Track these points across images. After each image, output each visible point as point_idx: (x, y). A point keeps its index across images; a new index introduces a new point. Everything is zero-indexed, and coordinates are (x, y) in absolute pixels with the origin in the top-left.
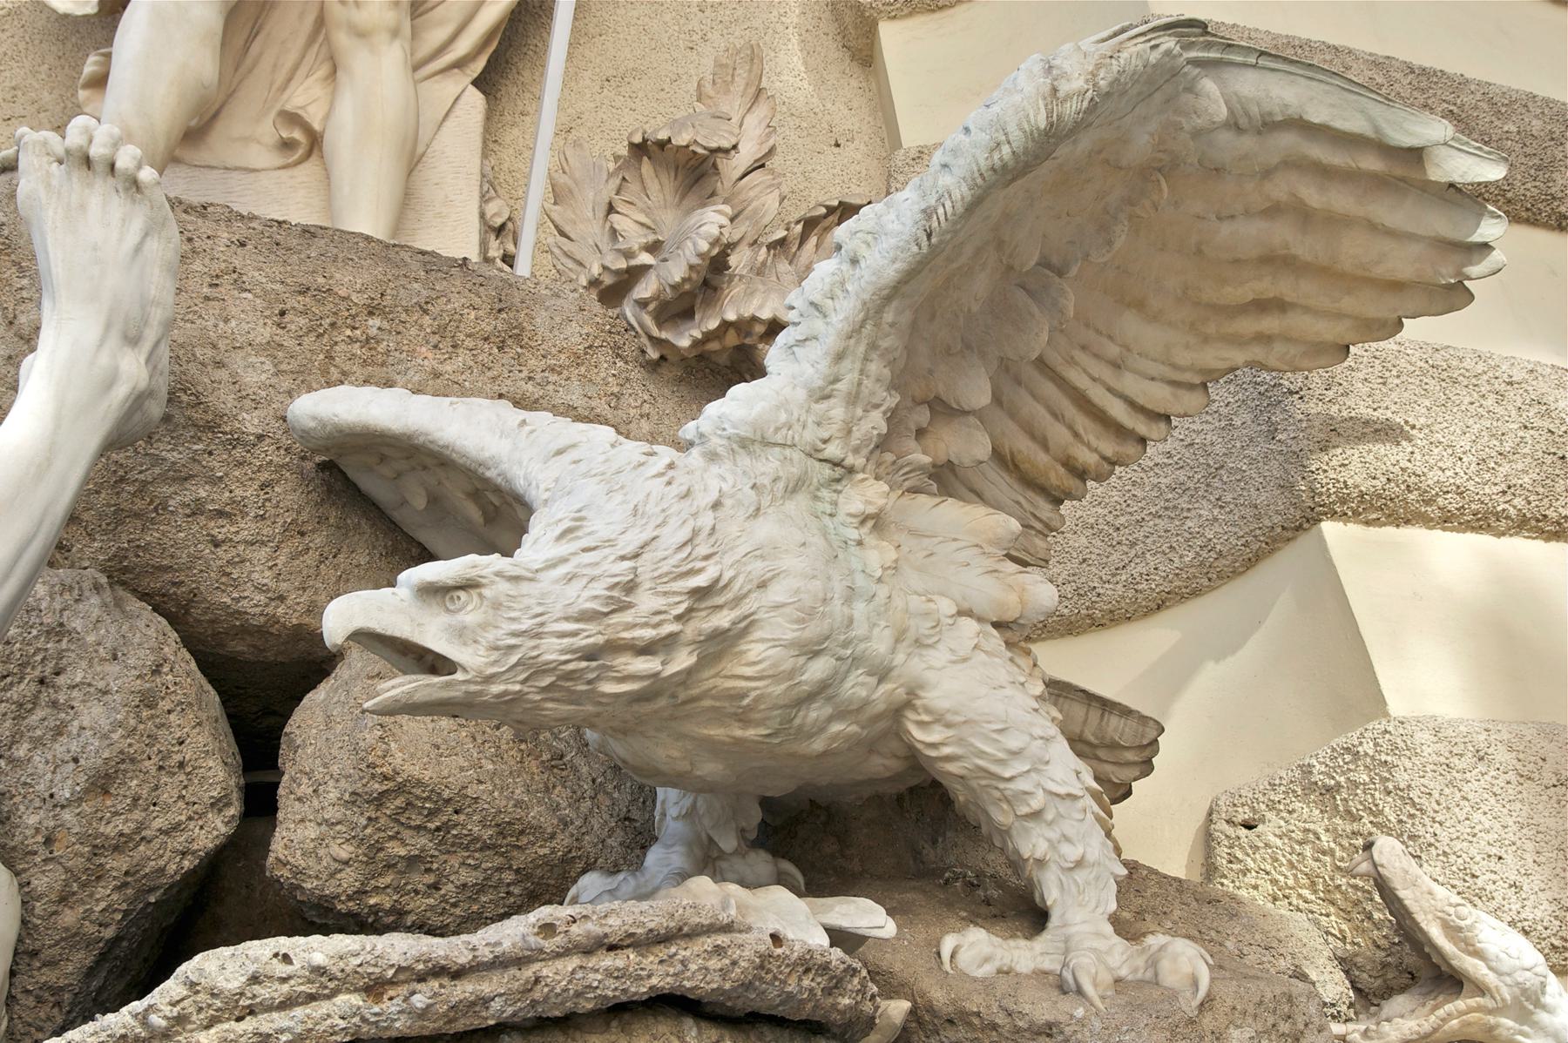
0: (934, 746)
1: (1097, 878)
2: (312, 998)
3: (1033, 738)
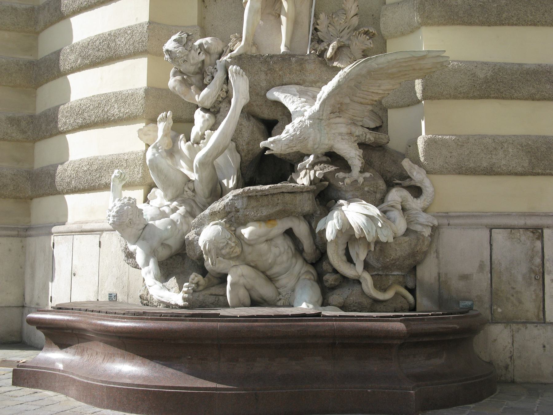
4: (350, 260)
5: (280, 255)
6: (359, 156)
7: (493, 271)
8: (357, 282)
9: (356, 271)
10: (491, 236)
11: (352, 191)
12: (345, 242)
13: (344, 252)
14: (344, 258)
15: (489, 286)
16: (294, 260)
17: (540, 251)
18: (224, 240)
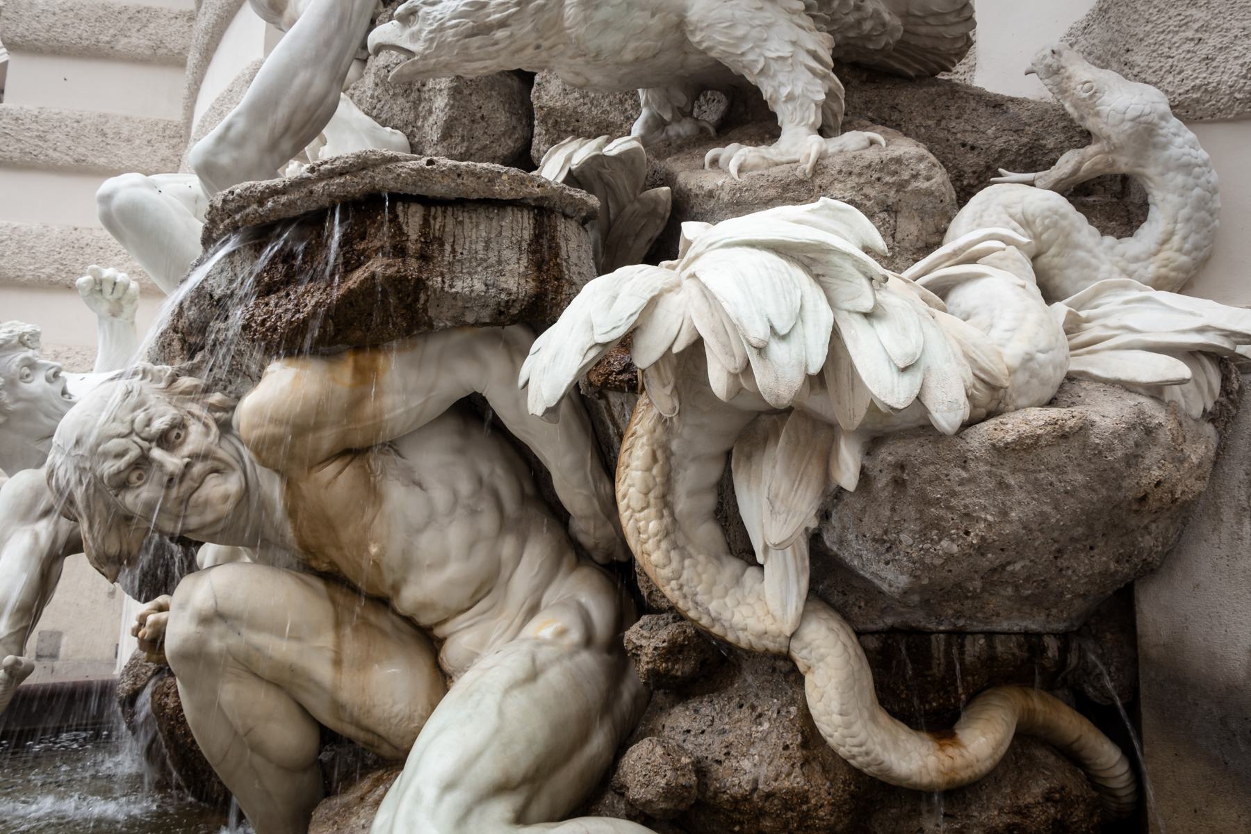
0: (700, 43)
1: (801, 105)
2: (244, 208)
3: (753, 27)
4: (740, 549)
5: (427, 525)
6: (815, 56)
8: (783, 670)
9: (763, 605)
12: (718, 447)
13: (710, 501)
14: (707, 532)
16: (508, 547)
18: (114, 445)
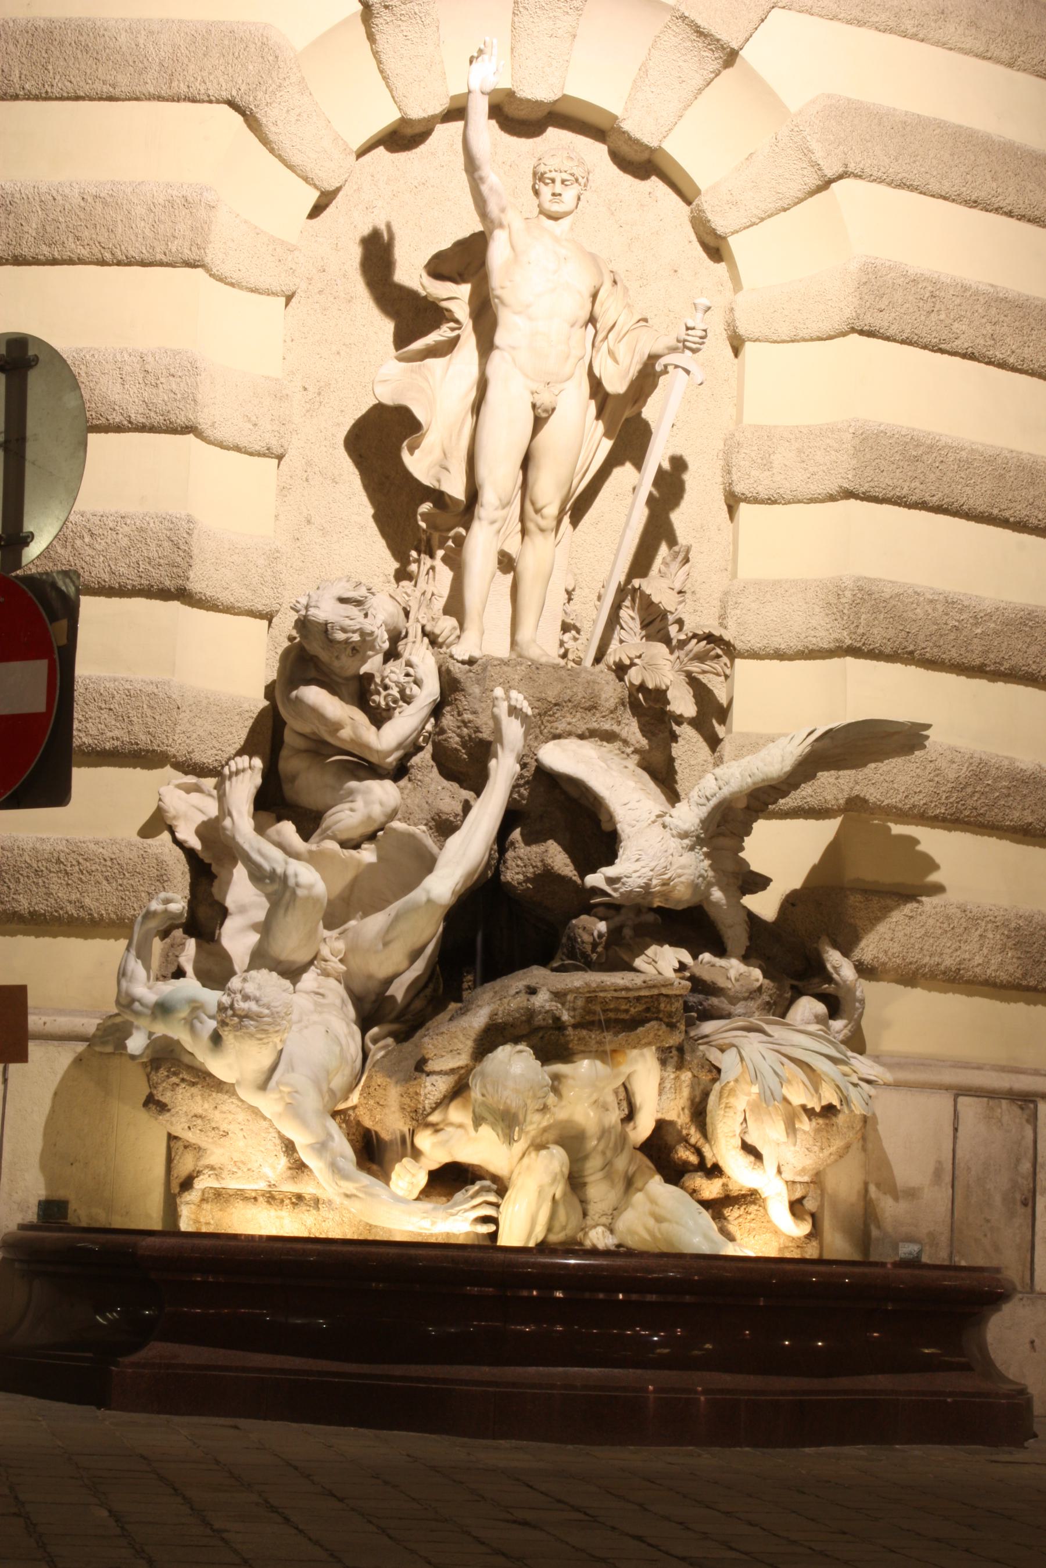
7: (956, 1183)
10: (955, 1110)
11: (745, 999)
15: (949, 1214)
17: (1031, 1145)
